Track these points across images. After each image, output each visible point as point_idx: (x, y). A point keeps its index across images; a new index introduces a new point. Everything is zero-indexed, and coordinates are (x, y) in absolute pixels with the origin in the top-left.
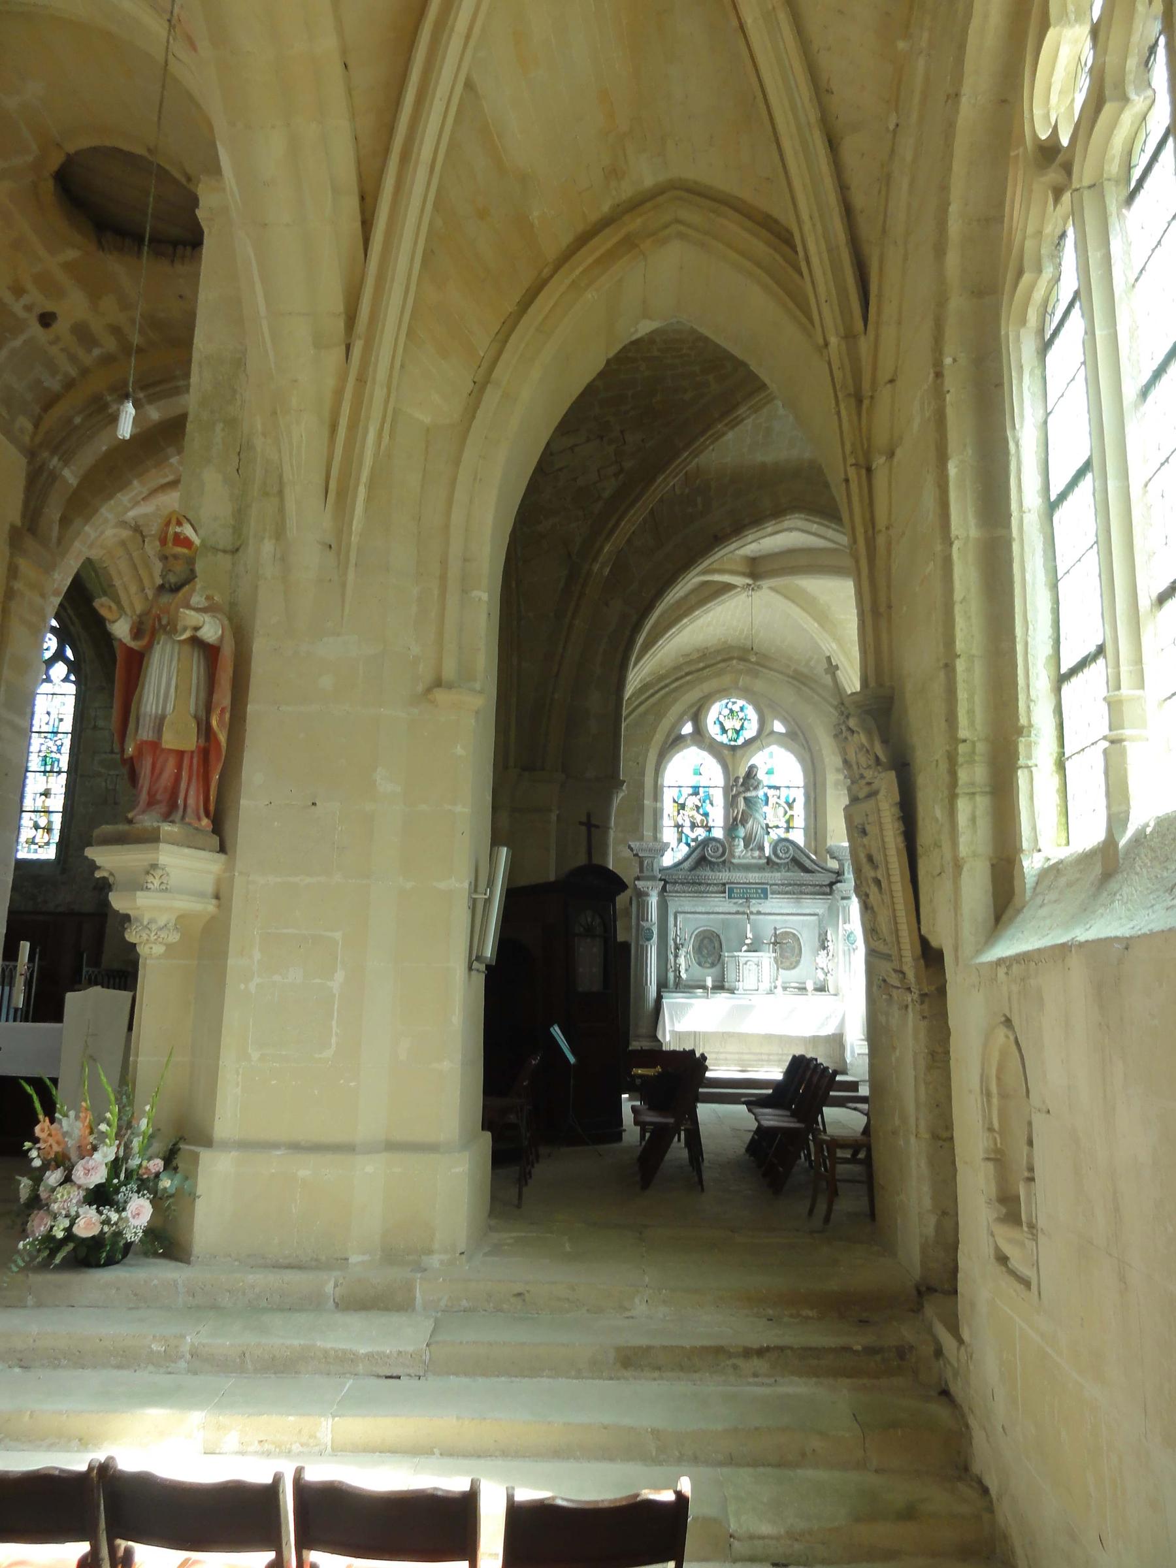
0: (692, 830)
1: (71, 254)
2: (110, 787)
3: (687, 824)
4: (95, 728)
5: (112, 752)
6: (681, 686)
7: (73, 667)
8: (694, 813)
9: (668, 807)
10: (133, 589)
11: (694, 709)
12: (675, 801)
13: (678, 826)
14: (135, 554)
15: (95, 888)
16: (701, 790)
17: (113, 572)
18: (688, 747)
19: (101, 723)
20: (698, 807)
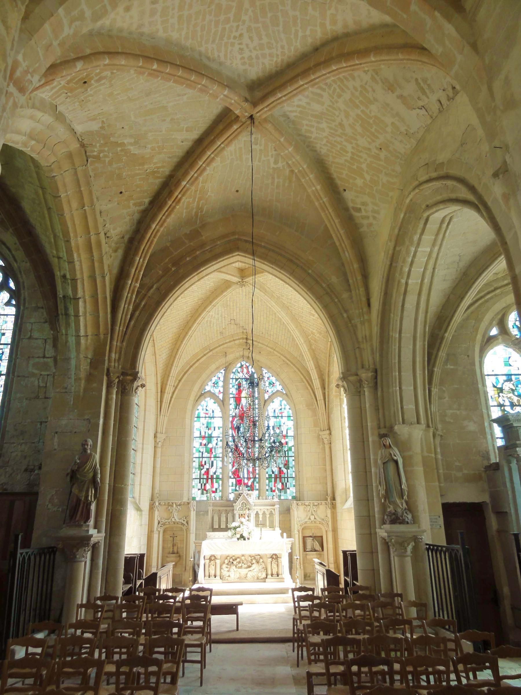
0: (512, 409)
2: (41, 384)
3: (507, 403)
4: (30, 338)
5: (44, 357)
6: (492, 298)
7: (13, 294)
8: (511, 395)
9: (491, 392)
10: (75, 205)
11: (499, 316)
12: (494, 386)
13: (500, 405)
14: (79, 169)
15: (26, 470)
16: (513, 377)
17: (60, 185)
18: (498, 344)
19: (36, 334)
20: (512, 390)
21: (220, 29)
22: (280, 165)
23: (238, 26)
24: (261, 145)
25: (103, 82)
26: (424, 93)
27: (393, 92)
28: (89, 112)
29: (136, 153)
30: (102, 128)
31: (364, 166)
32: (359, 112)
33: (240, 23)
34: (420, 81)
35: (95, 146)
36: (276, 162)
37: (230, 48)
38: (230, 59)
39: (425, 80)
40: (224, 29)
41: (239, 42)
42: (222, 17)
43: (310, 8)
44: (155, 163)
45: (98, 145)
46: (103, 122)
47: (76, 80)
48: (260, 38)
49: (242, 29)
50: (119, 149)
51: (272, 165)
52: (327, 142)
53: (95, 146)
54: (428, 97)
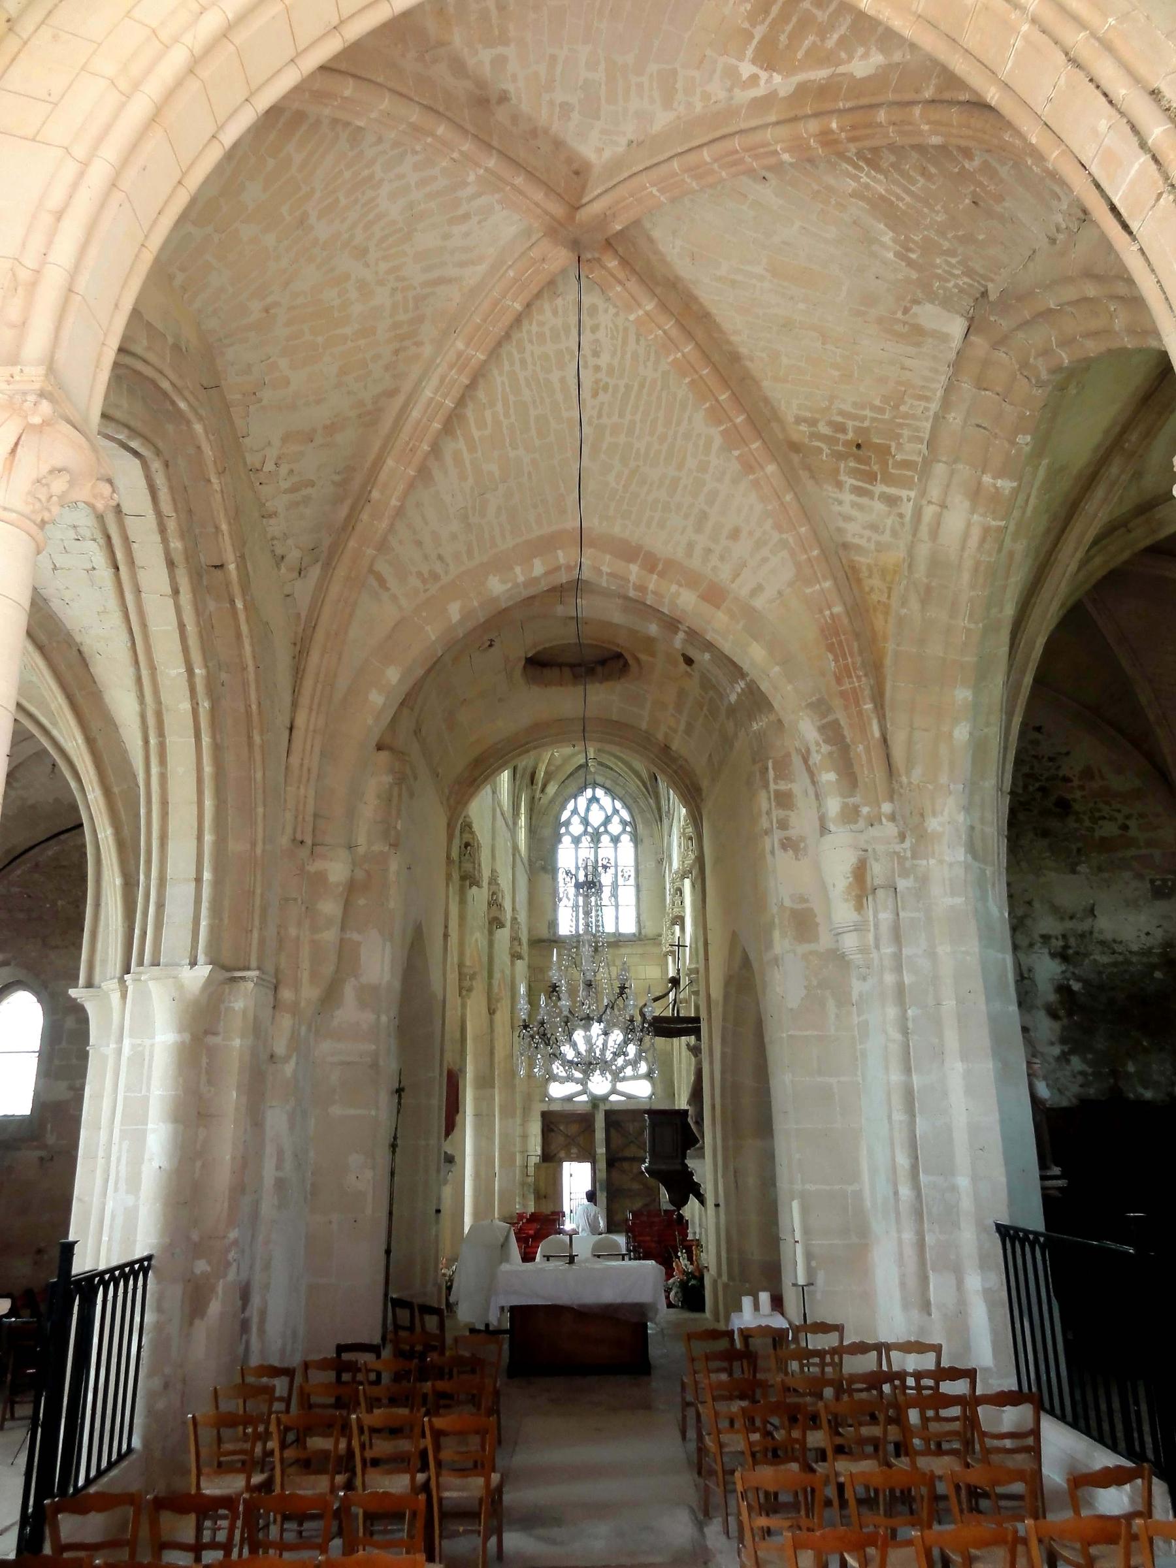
1: (643, 657)
21: (628, 417)
22: (486, 56)
23: (600, 416)
24: (551, 103)
25: (840, 419)
26: (294, 489)
27: (325, 427)
28: (908, 362)
29: (882, 226)
30: (916, 302)
31: (270, 239)
32: (348, 330)
33: (595, 421)
34: (309, 491)
35: (956, 286)
36: (500, 62)
37: (616, 362)
38: (616, 326)
39: (306, 500)
40: (621, 415)
41: (599, 376)
42: (622, 439)
43: (497, 474)
44: (856, 178)
45: (950, 285)
46: (906, 311)
47: (863, 467)
48: (562, 380)
49: (593, 407)
50: (913, 256)
51: (510, 51)
52: (371, 177)
53: (956, 286)
54: (285, 492)
